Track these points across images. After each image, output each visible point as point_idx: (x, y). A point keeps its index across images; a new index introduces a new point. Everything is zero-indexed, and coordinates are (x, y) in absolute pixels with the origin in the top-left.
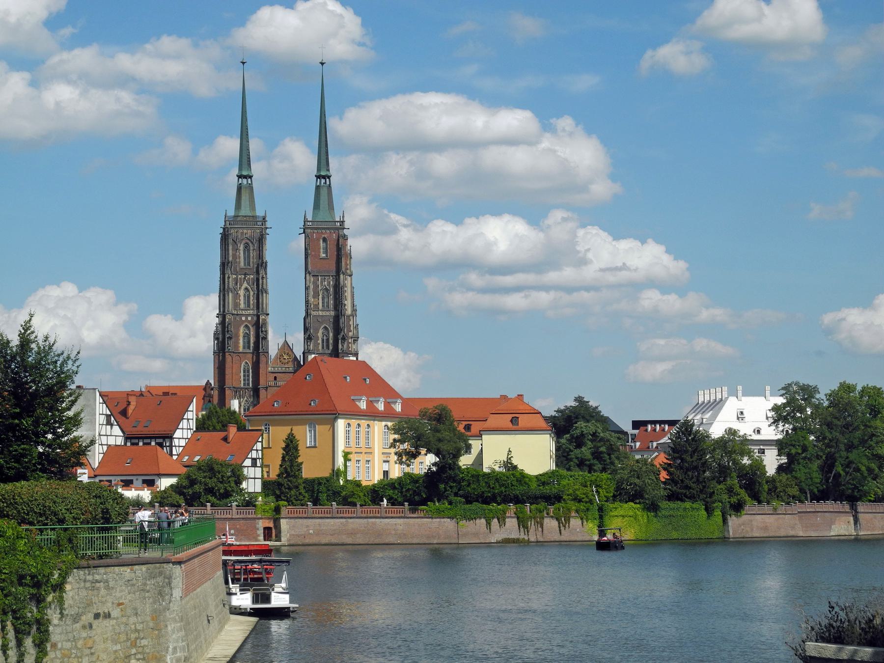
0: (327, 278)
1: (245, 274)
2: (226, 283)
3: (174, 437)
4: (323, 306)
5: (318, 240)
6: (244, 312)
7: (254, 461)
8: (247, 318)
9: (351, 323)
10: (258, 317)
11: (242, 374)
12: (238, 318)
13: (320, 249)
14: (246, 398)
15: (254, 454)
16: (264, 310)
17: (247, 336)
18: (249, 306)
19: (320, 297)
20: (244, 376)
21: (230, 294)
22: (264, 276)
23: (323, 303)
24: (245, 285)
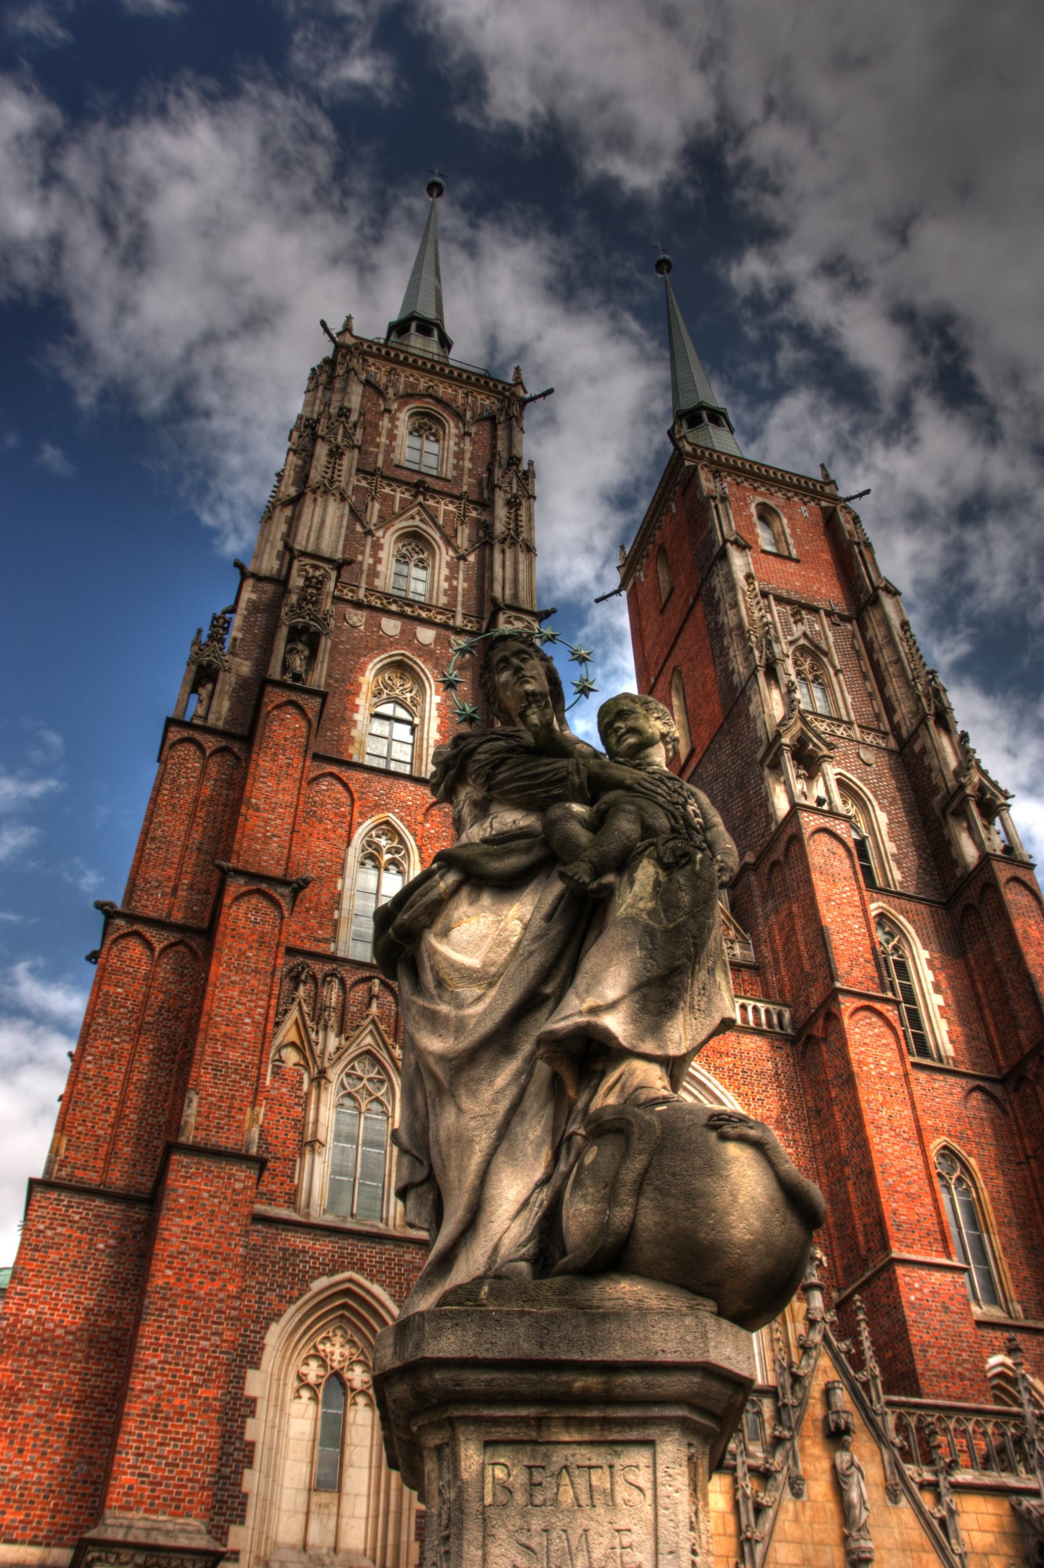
6: (394, 608)
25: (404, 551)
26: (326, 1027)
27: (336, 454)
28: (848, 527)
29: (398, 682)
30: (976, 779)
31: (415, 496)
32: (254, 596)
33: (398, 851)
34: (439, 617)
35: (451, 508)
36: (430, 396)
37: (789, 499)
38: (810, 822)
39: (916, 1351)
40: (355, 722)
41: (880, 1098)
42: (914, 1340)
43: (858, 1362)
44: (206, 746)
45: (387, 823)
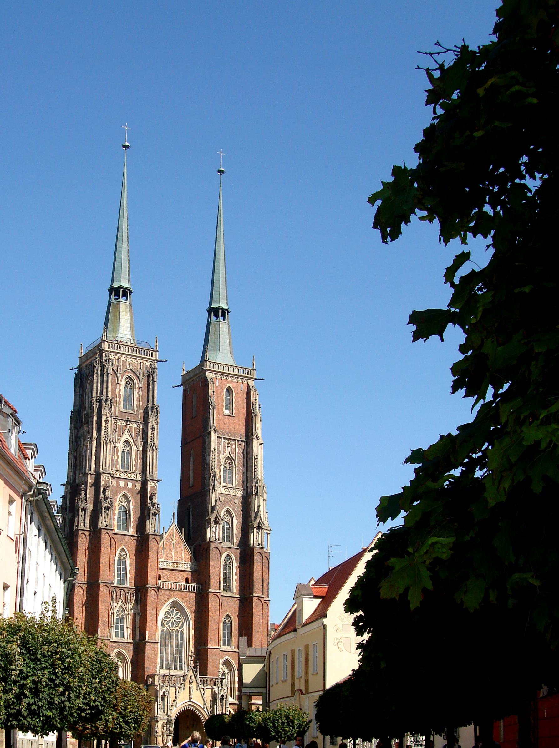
0: (231, 442)
1: (127, 421)
2: (103, 428)
4: (225, 482)
5: (222, 389)
6: (122, 475)
8: (126, 485)
11: (116, 566)
14: (120, 603)
20: (119, 569)
22: (155, 426)
24: (126, 436)
25: (124, 448)
26: (114, 603)
27: (107, 421)
28: (252, 399)
29: (123, 499)
30: (258, 521)
31: (127, 425)
32: (91, 481)
33: (125, 555)
34: (133, 475)
35: (136, 426)
36: (130, 369)
37: (237, 382)
38: (212, 545)
39: (208, 663)
40: (115, 519)
41: (213, 615)
42: (208, 661)
43: (196, 672)
44: (86, 534)
45: (123, 548)
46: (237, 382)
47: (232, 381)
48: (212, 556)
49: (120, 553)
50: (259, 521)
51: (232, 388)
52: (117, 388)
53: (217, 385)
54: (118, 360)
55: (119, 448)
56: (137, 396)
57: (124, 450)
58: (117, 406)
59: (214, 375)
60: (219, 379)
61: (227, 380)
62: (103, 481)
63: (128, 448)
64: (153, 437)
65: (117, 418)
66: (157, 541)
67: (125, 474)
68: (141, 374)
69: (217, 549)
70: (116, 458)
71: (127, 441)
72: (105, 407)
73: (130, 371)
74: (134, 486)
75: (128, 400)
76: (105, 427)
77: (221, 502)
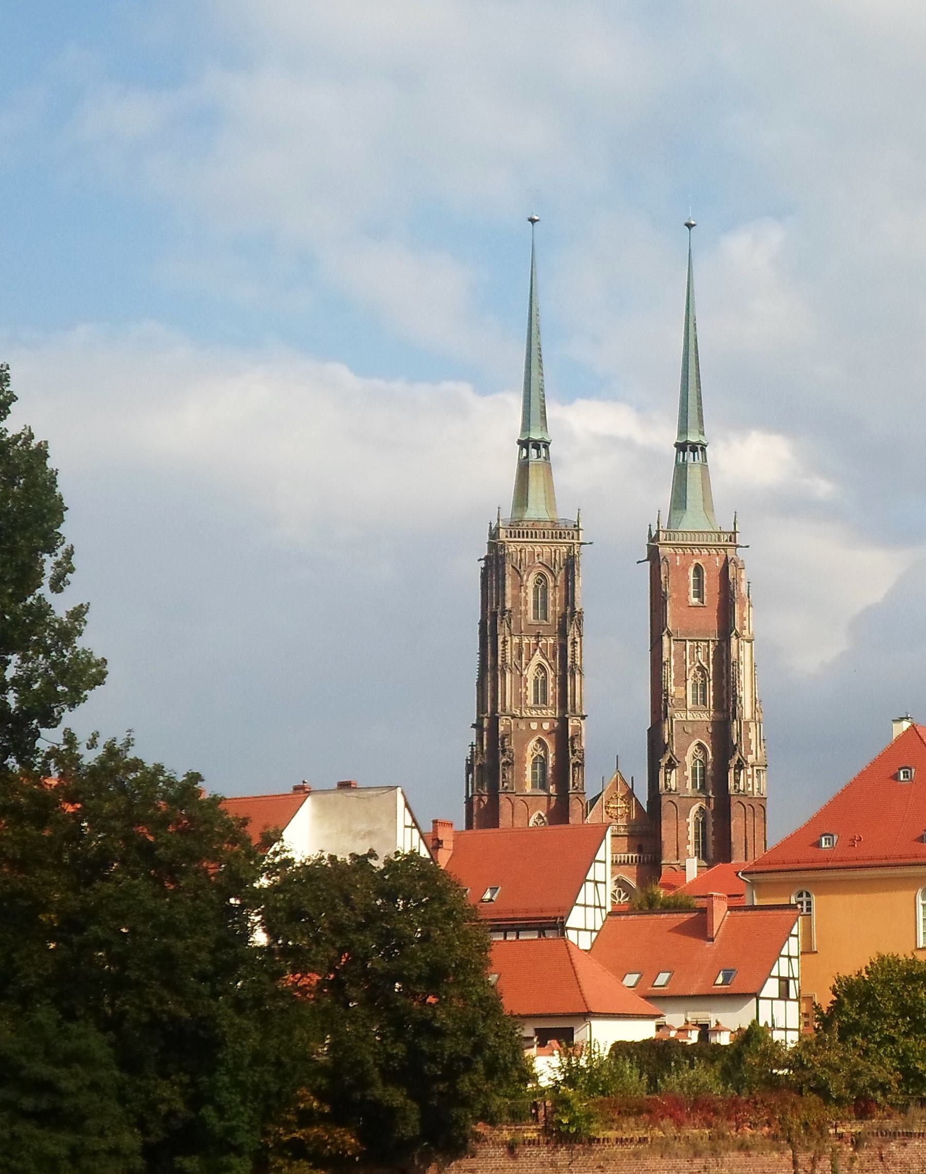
1: (538, 636)
2: (500, 653)
3: (567, 925)
4: (695, 702)
6: (534, 712)
7: (784, 982)
9: (752, 735)
10: (564, 722)
12: (522, 726)
13: (688, 586)
15: (782, 968)
16: (578, 710)
17: (540, 762)
18: (545, 701)
19: (690, 683)
21: (508, 676)
22: (578, 640)
23: (695, 696)
24: (537, 658)
27: (504, 642)
29: (539, 745)
30: (737, 758)
34: (550, 711)
36: (540, 562)
37: (710, 555)
45: (539, 814)
46: (710, 555)
47: (701, 555)
48: (664, 814)
49: (536, 820)
50: (739, 758)
51: (701, 564)
52: (521, 592)
53: (678, 564)
54: (520, 551)
55: (527, 676)
56: (552, 598)
57: (536, 677)
58: (523, 617)
59: (671, 549)
60: (680, 555)
61: (693, 554)
62: (502, 727)
63: (543, 674)
64: (574, 655)
65: (523, 634)
66: (580, 801)
67: (539, 711)
68: (556, 567)
69: (673, 805)
70: (524, 690)
71: (540, 665)
72: (502, 622)
73: (539, 565)
74: (552, 725)
75: (541, 604)
76: (503, 650)
77: (686, 733)
